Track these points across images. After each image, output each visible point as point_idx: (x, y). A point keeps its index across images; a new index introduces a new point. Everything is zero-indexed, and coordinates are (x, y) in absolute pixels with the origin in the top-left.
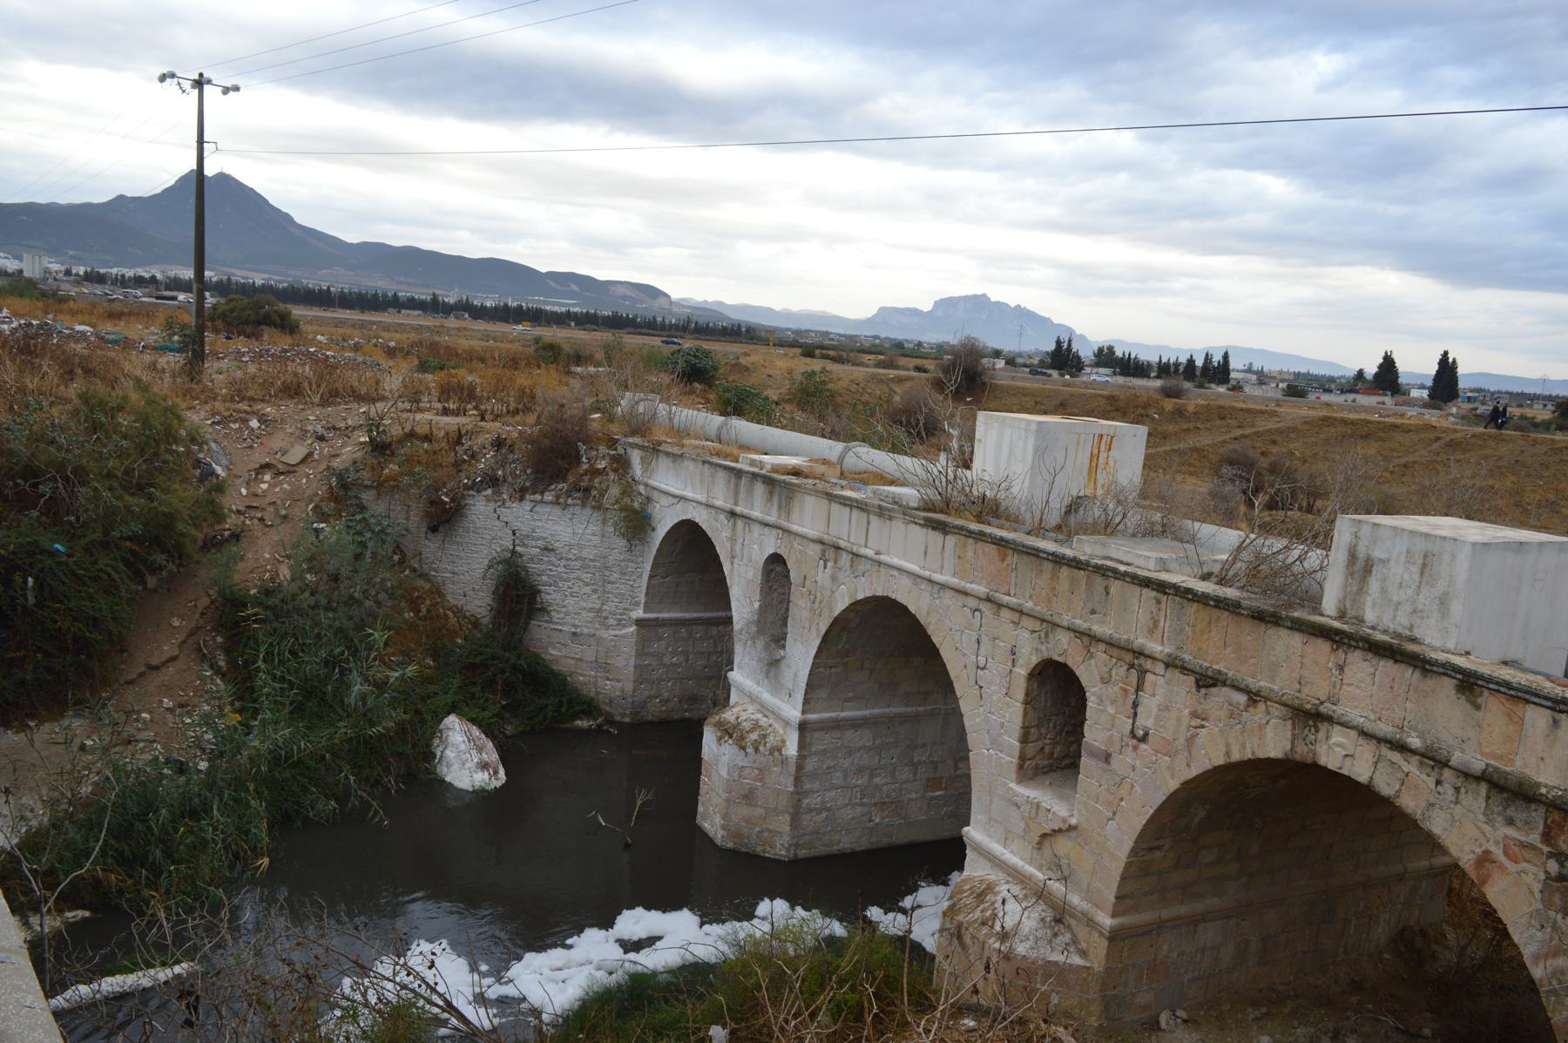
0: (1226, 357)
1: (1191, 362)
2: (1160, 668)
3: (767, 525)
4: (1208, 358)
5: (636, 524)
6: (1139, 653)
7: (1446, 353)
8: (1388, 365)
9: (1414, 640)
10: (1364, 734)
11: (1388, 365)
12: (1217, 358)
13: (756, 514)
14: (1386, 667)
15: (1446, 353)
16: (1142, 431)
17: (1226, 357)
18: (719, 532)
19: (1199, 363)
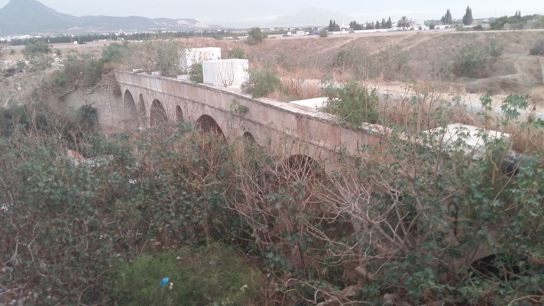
0: (390, 18)
1: (378, 22)
2: (188, 102)
3: (138, 87)
4: (383, 20)
5: (117, 93)
6: (186, 99)
7: (468, 7)
8: (448, 14)
9: (212, 85)
10: (209, 106)
11: (448, 14)
12: (386, 20)
13: (136, 84)
14: (209, 91)
15: (468, 7)
16: (219, 49)
17: (390, 18)
18: (132, 90)
19: (380, 22)
